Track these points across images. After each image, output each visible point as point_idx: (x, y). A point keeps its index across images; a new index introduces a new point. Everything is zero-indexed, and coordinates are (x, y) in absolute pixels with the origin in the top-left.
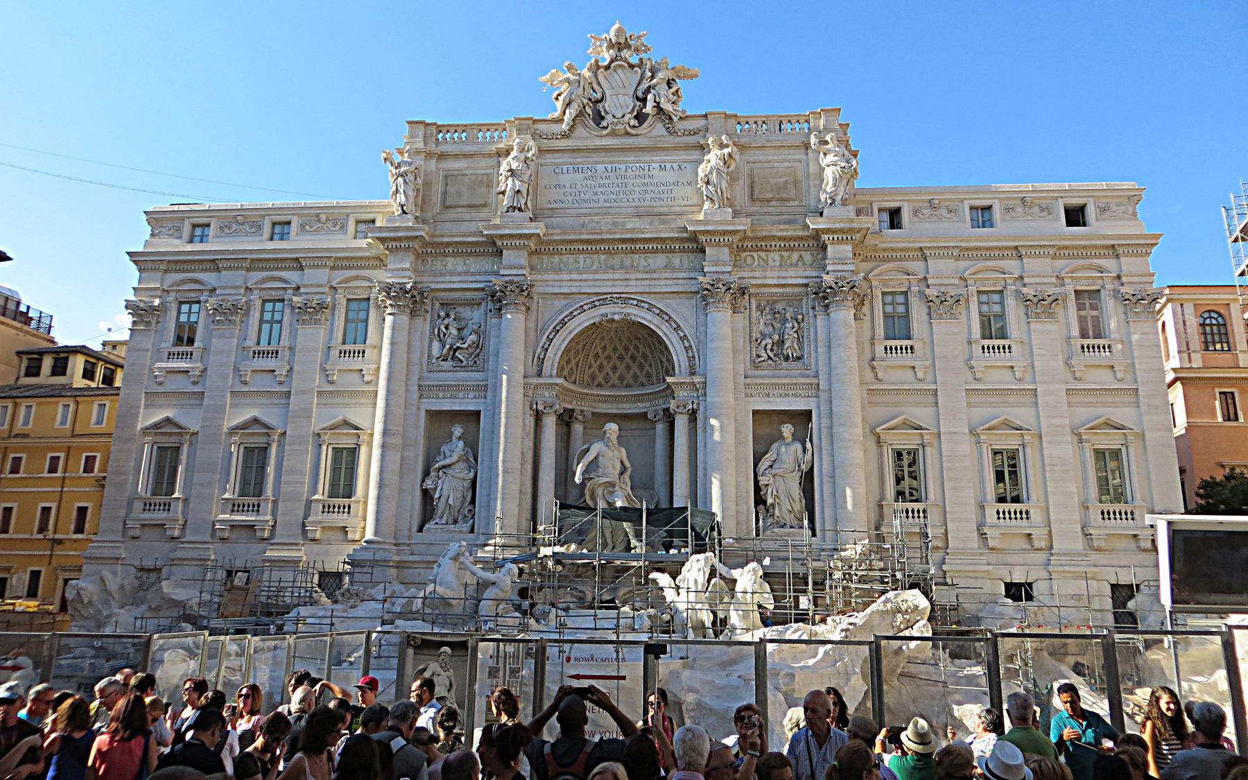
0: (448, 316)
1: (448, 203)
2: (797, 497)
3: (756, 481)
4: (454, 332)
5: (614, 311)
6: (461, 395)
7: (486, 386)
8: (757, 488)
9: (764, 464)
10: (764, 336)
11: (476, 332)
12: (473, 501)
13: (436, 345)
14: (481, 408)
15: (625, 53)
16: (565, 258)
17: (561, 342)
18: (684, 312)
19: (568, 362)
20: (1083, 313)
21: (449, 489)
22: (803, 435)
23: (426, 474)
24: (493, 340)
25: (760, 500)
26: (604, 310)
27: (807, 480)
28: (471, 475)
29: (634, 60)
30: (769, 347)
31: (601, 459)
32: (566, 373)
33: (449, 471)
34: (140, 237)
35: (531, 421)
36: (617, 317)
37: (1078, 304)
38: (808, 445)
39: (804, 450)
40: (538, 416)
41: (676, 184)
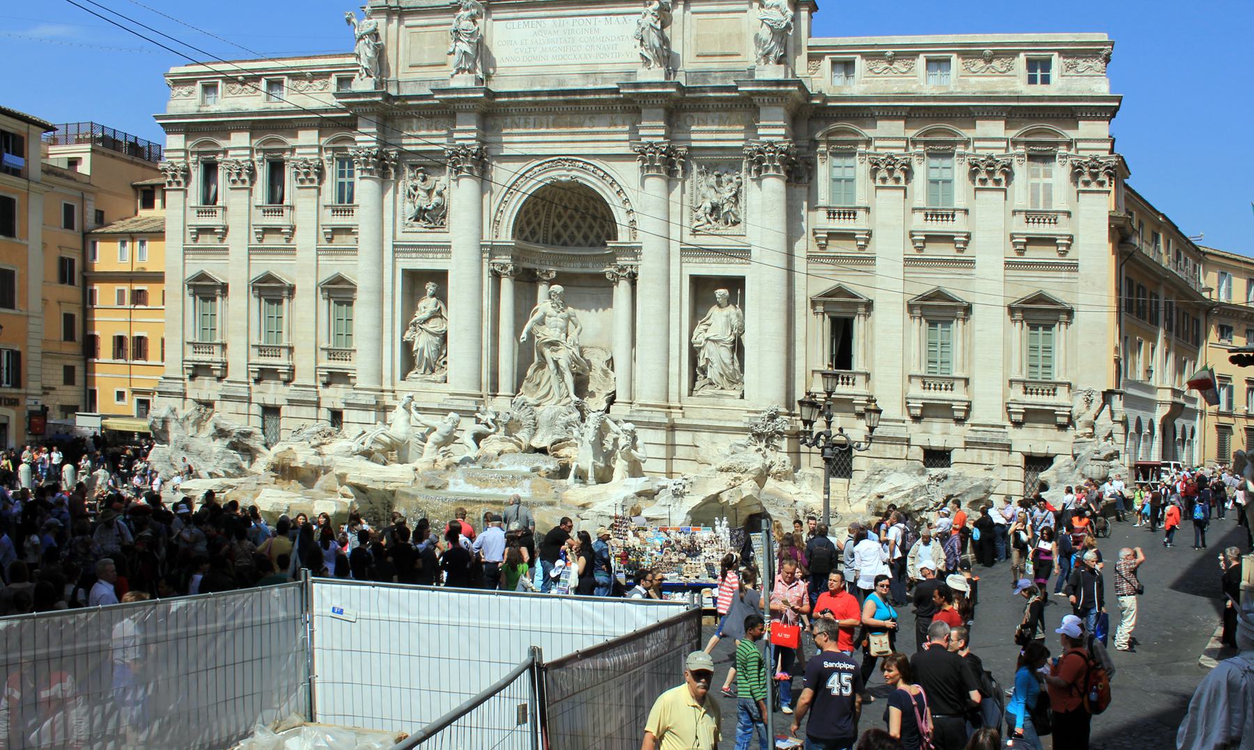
1: (413, 63)
2: (728, 361)
4: (422, 193)
5: (562, 174)
6: (431, 255)
7: (450, 247)
11: (440, 194)
13: (409, 206)
16: (516, 118)
17: (516, 203)
18: (628, 173)
19: (529, 223)
21: (423, 343)
26: (554, 174)
27: (738, 348)
30: (708, 210)
31: (547, 319)
32: (527, 233)
33: (424, 326)
36: (563, 179)
40: (496, 276)
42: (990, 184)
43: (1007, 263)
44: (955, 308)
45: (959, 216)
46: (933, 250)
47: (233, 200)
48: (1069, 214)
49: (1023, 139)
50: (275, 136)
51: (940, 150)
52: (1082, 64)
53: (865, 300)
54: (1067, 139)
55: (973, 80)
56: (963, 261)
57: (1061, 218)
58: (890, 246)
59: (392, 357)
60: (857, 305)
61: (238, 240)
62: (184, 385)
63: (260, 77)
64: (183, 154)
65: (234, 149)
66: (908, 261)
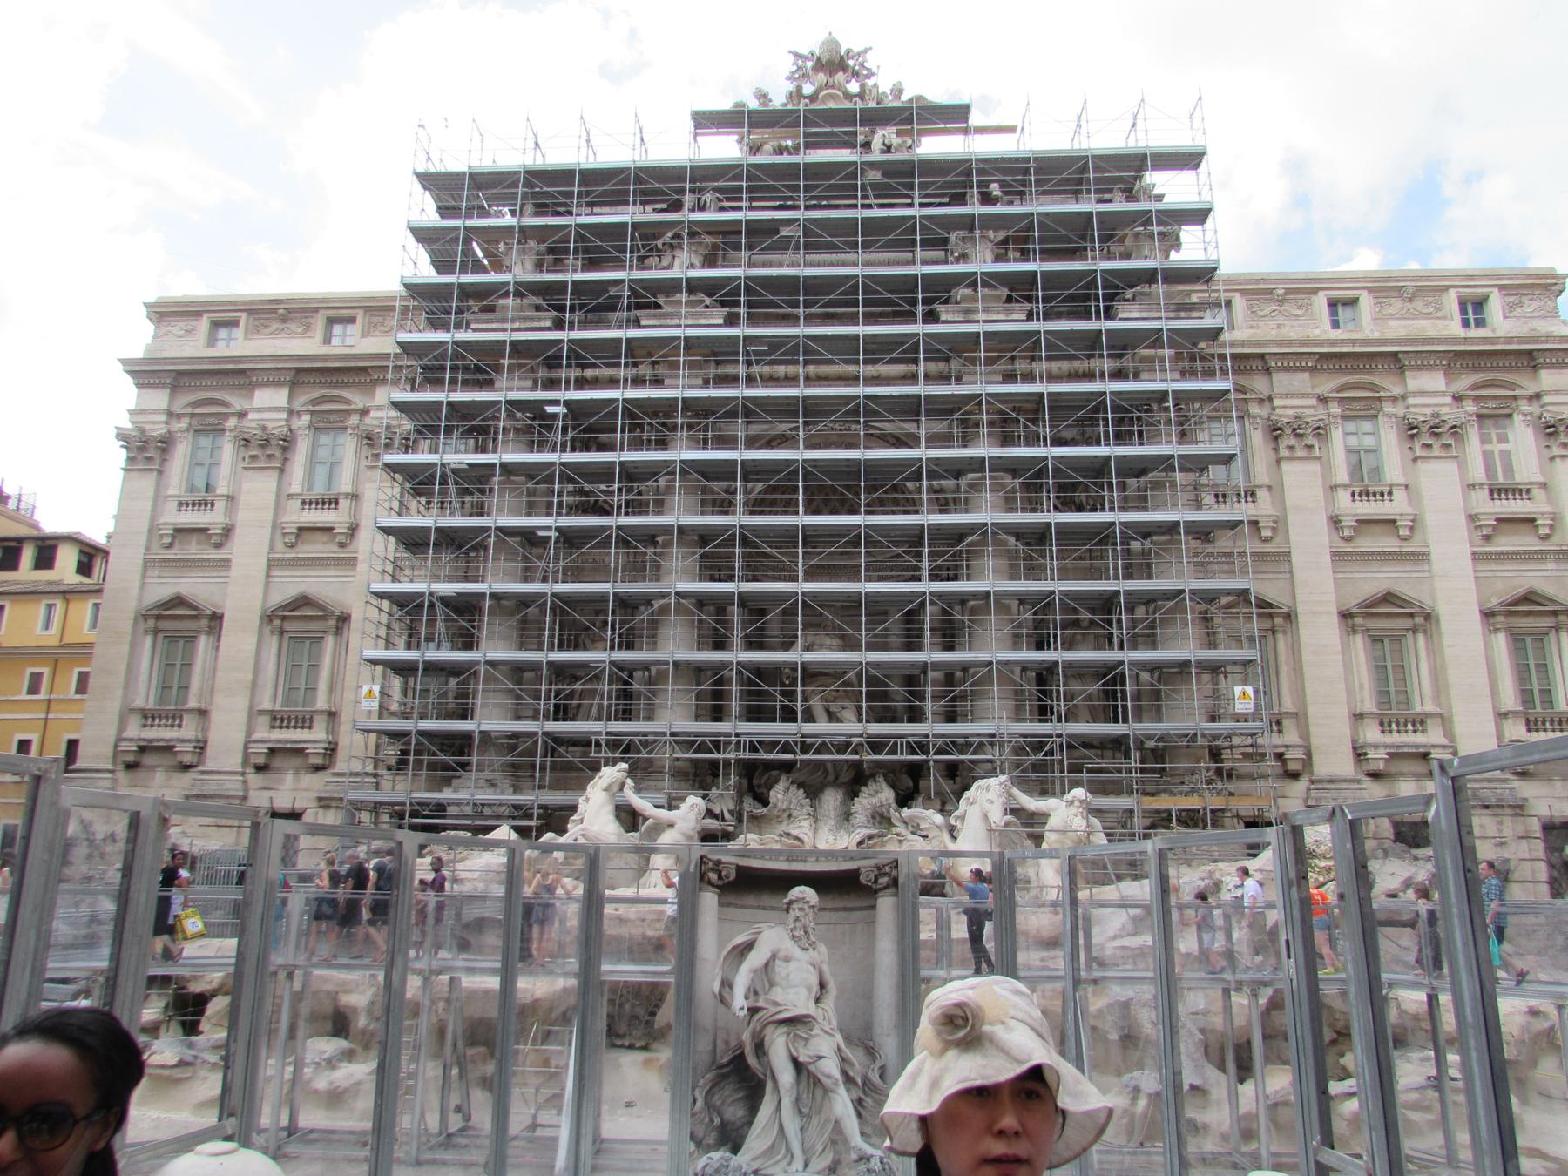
15: (840, 77)
20: (1488, 447)
29: (854, 87)
34: (139, 338)
37: (1482, 435)
42: (1436, 451)
43: (1474, 553)
44: (1411, 615)
45: (1398, 494)
46: (1366, 544)
47: (246, 486)
48: (1544, 486)
49: (1470, 393)
50: (335, 392)
51: (1364, 408)
52: (1530, 306)
53: (1285, 610)
54: (1530, 392)
55: (1393, 323)
56: (1413, 553)
57: (1536, 492)
58: (1309, 543)
60: (1271, 616)
61: (250, 551)
62: (115, 780)
63: (316, 310)
64: (163, 418)
65: (260, 410)
66: (1338, 557)
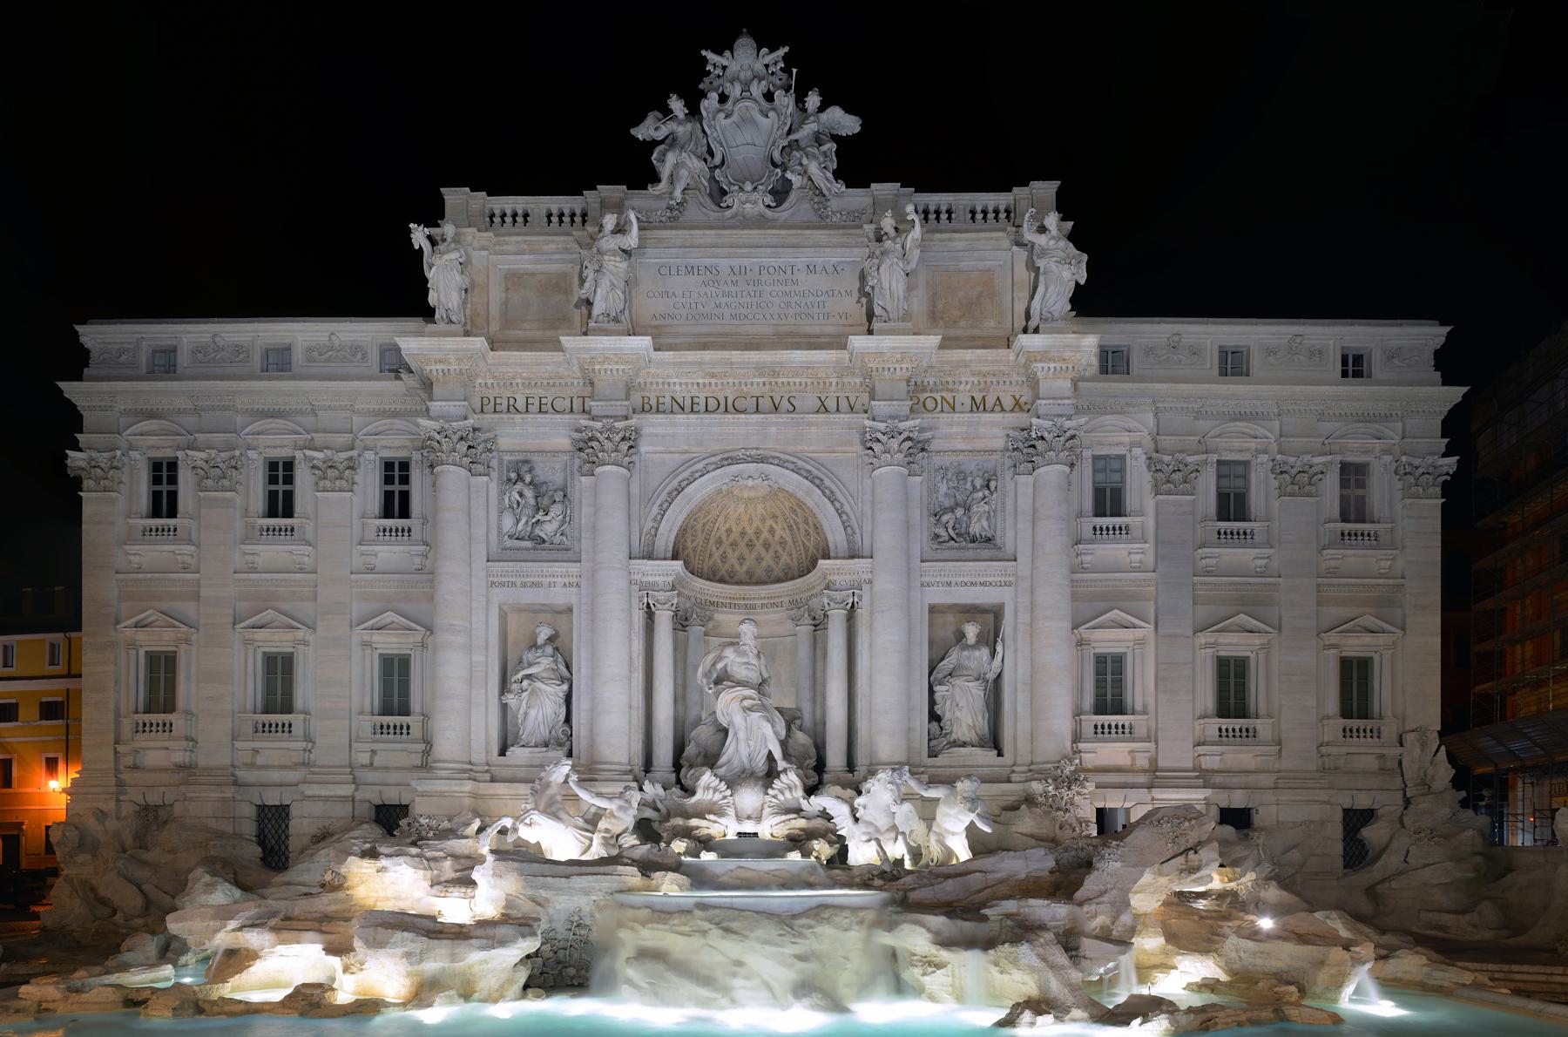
0: (520, 478)
3: (931, 692)
4: (532, 501)
8: (932, 702)
9: (937, 675)
10: (945, 511)
12: (568, 720)
13: (508, 523)
14: (574, 601)
22: (991, 638)
23: (504, 687)
24: (586, 510)
25: (934, 717)
28: (565, 687)
35: (639, 617)
38: (999, 648)
39: (993, 653)
40: (650, 615)
41: (830, 293)
59: (486, 729)
